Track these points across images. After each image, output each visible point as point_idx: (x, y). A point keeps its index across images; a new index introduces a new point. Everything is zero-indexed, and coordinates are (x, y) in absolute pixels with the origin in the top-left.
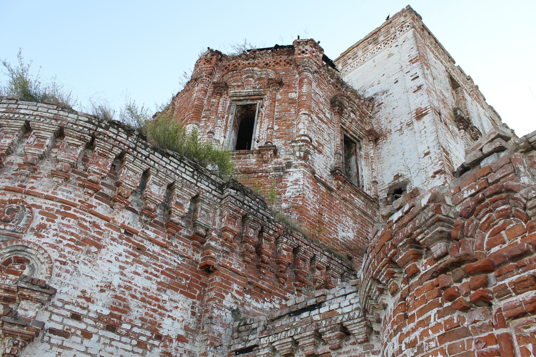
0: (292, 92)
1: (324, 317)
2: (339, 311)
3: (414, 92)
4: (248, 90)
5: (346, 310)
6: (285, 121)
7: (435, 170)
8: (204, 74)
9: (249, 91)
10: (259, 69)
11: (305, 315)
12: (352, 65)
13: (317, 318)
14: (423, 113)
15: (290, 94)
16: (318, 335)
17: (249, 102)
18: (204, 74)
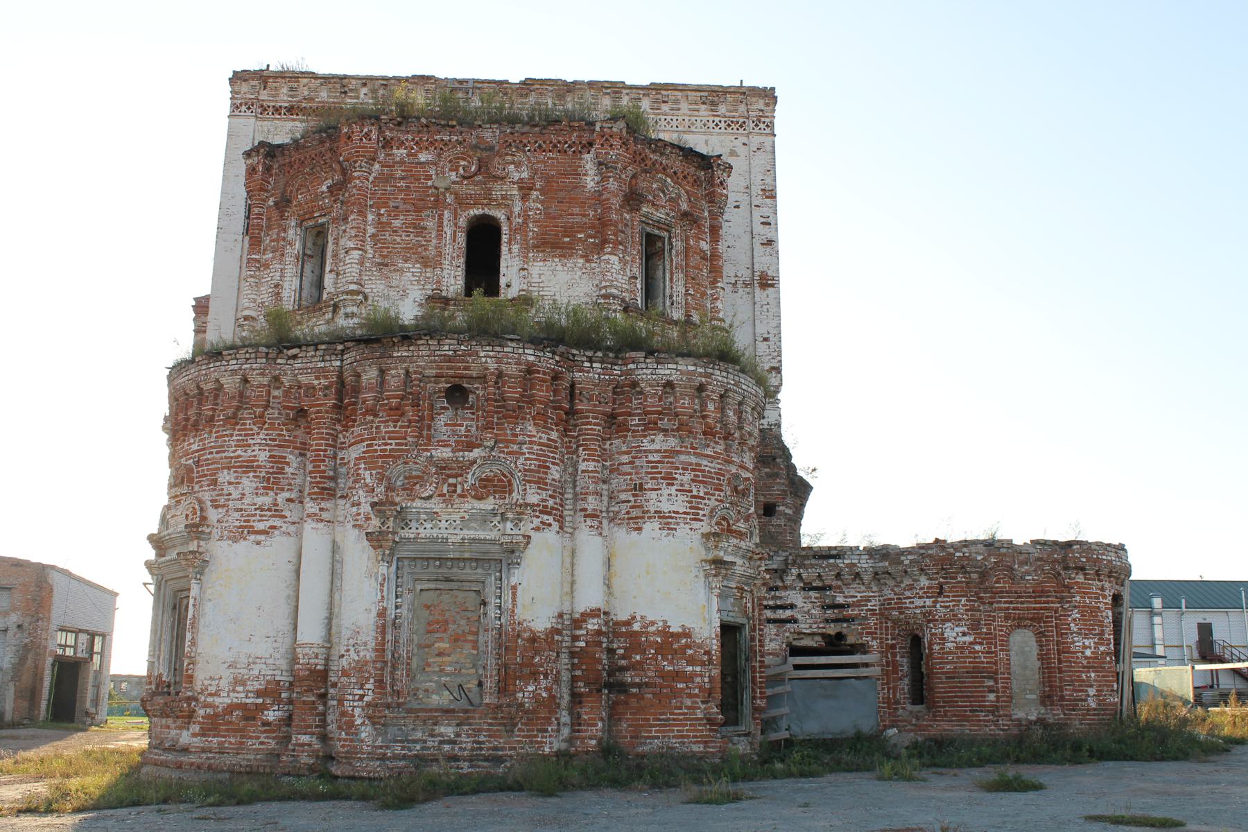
0: (703, 240)
1: (847, 566)
2: (859, 565)
3: (762, 244)
4: (661, 215)
5: (865, 565)
6: (698, 284)
7: (772, 365)
8: (619, 165)
9: (661, 216)
10: (673, 184)
11: (832, 561)
12: (669, 118)
13: (841, 565)
14: (769, 282)
15: (701, 242)
16: (838, 576)
17: (657, 232)
18: (619, 165)
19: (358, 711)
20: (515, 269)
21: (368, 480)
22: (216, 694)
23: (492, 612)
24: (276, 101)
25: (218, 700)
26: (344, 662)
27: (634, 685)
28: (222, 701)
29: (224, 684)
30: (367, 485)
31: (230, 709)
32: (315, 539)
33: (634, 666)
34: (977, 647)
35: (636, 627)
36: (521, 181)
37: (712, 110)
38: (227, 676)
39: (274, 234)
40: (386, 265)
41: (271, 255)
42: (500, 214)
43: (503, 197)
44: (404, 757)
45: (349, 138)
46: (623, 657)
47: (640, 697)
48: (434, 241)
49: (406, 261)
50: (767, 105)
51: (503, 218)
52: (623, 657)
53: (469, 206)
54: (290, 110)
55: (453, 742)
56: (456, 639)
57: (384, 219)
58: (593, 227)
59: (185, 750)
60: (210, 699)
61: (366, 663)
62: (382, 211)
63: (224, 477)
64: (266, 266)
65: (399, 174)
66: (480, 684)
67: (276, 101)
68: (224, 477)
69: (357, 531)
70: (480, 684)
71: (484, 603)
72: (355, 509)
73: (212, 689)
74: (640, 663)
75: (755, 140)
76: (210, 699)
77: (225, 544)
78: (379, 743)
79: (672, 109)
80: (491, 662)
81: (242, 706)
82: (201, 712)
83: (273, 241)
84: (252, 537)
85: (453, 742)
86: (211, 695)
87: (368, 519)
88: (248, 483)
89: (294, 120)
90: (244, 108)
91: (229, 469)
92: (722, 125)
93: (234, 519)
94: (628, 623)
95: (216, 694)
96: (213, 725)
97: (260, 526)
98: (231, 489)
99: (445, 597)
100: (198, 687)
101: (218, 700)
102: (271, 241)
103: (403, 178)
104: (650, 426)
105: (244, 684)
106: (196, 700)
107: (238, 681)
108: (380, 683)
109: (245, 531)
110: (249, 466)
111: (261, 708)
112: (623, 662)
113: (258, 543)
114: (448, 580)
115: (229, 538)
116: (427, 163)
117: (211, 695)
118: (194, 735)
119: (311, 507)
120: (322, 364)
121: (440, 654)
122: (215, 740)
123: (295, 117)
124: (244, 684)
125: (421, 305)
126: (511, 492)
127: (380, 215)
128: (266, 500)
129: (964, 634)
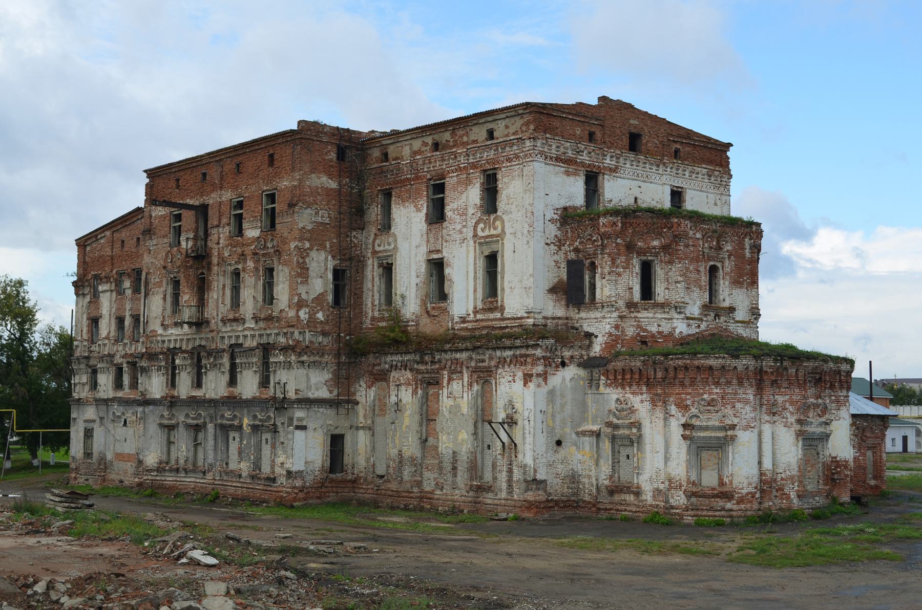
19: (791, 493)
20: (727, 293)
21: (791, 410)
22: (742, 489)
23: (821, 457)
24: (551, 153)
25: (743, 491)
26: (783, 475)
27: (838, 479)
28: (744, 491)
29: (745, 485)
30: (791, 412)
31: (748, 494)
32: (767, 429)
33: (838, 473)
34: (860, 458)
35: (838, 459)
36: (728, 251)
37: (709, 179)
38: (746, 482)
39: (623, 258)
40: (688, 288)
41: (622, 270)
42: (719, 265)
43: (722, 258)
44: (809, 509)
45: (679, 225)
46: (834, 469)
47: (839, 483)
48: (703, 278)
49: (695, 286)
50: (728, 179)
51: (720, 268)
52: (834, 469)
53: (711, 260)
54: (558, 159)
55: (818, 502)
56: (812, 466)
57: (687, 266)
58: (749, 275)
59: (731, 510)
60: (739, 491)
61: (794, 476)
62: (687, 262)
63: (738, 405)
64: (619, 275)
65: (691, 243)
66: (818, 482)
67: (551, 153)
68: (738, 405)
69: (787, 428)
70: (818, 482)
71: (818, 454)
72: (784, 420)
73: (741, 487)
74: (839, 472)
75: (724, 198)
76: (739, 491)
77: (742, 431)
78: (800, 504)
79: (696, 177)
80: (821, 474)
81: (751, 493)
82: (737, 496)
83: (623, 262)
84: (750, 429)
85: (818, 502)
86: (740, 489)
87: (792, 424)
88: (748, 408)
89: (559, 166)
90: (539, 156)
91: (740, 402)
92: (712, 188)
93: (744, 423)
94: (836, 458)
95: (742, 489)
96: (740, 501)
97: (752, 425)
98: (742, 410)
99: (808, 451)
100: (734, 486)
101: (743, 491)
102: (621, 262)
103: (692, 246)
104: (841, 388)
105: (751, 485)
106: (735, 491)
107: (750, 484)
108: (801, 482)
109: (747, 427)
110: (747, 402)
111: (755, 493)
112: (834, 471)
113: (752, 431)
114: (811, 446)
115: (742, 430)
116: (699, 239)
117: (740, 489)
118: (734, 504)
119: (767, 418)
120: (773, 364)
121: (809, 472)
122: (743, 506)
123: (558, 164)
124: (751, 485)
125: (700, 308)
126: (825, 414)
127: (686, 263)
128: (752, 415)
129: (856, 453)
